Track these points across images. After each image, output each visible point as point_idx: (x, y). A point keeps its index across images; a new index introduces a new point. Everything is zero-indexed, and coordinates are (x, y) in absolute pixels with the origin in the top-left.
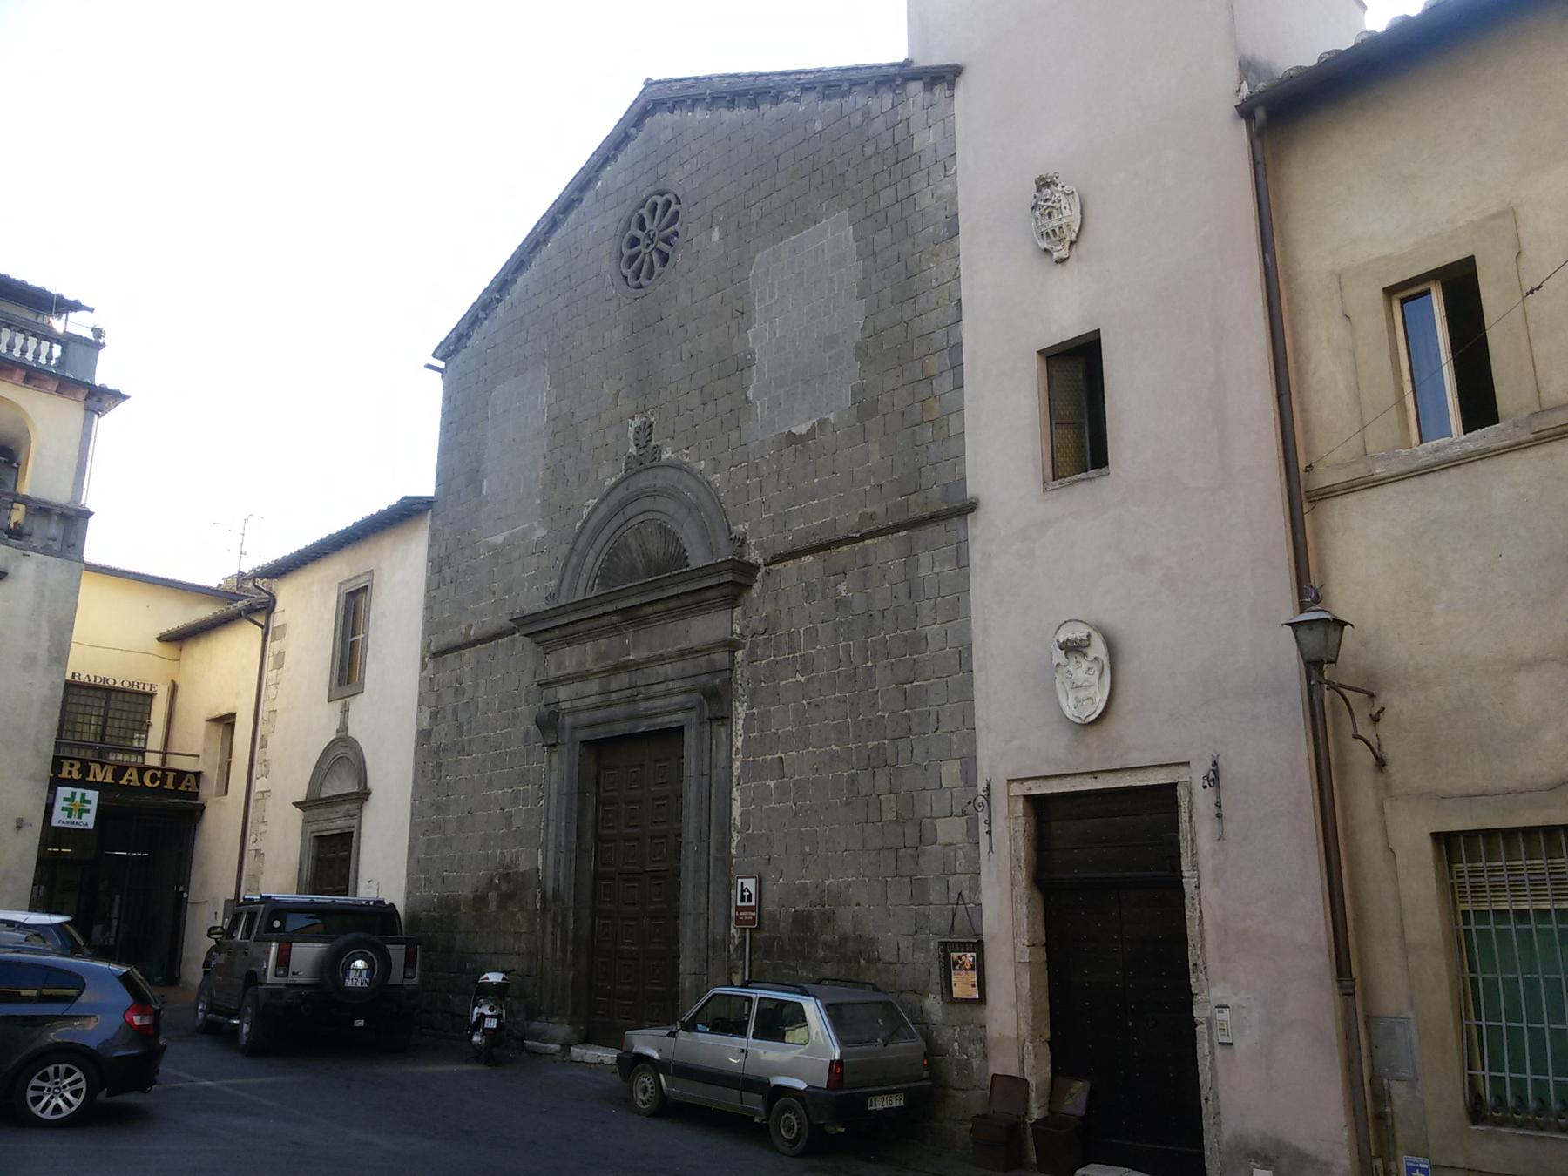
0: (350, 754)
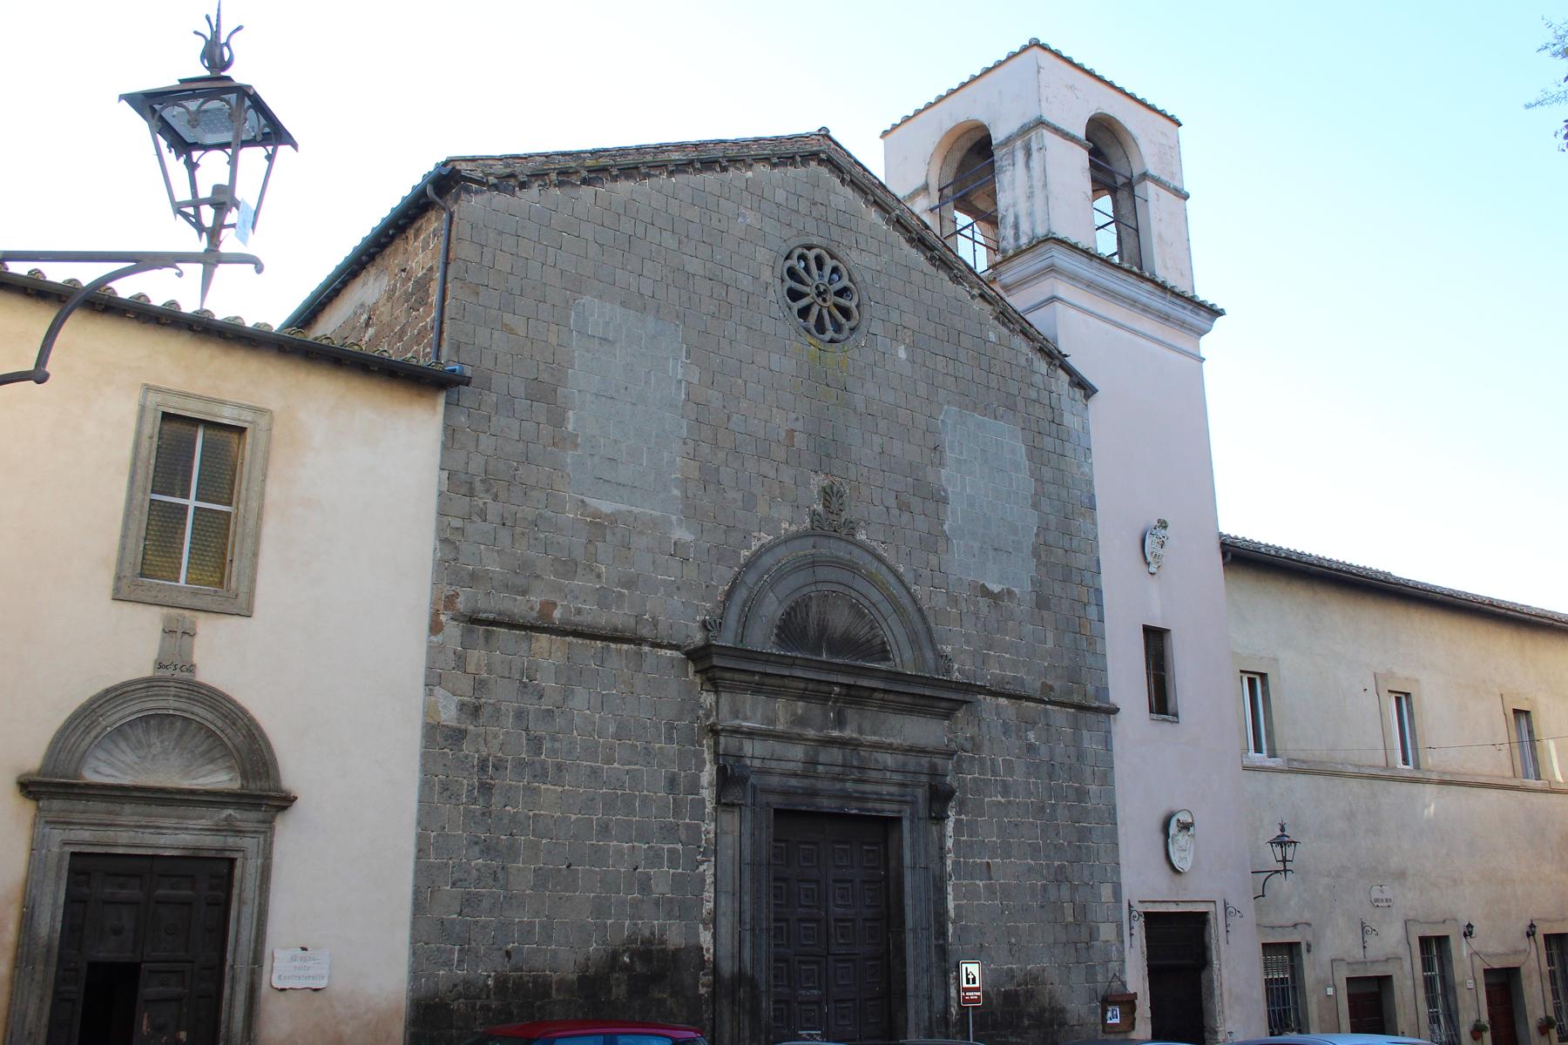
0: (201, 713)
